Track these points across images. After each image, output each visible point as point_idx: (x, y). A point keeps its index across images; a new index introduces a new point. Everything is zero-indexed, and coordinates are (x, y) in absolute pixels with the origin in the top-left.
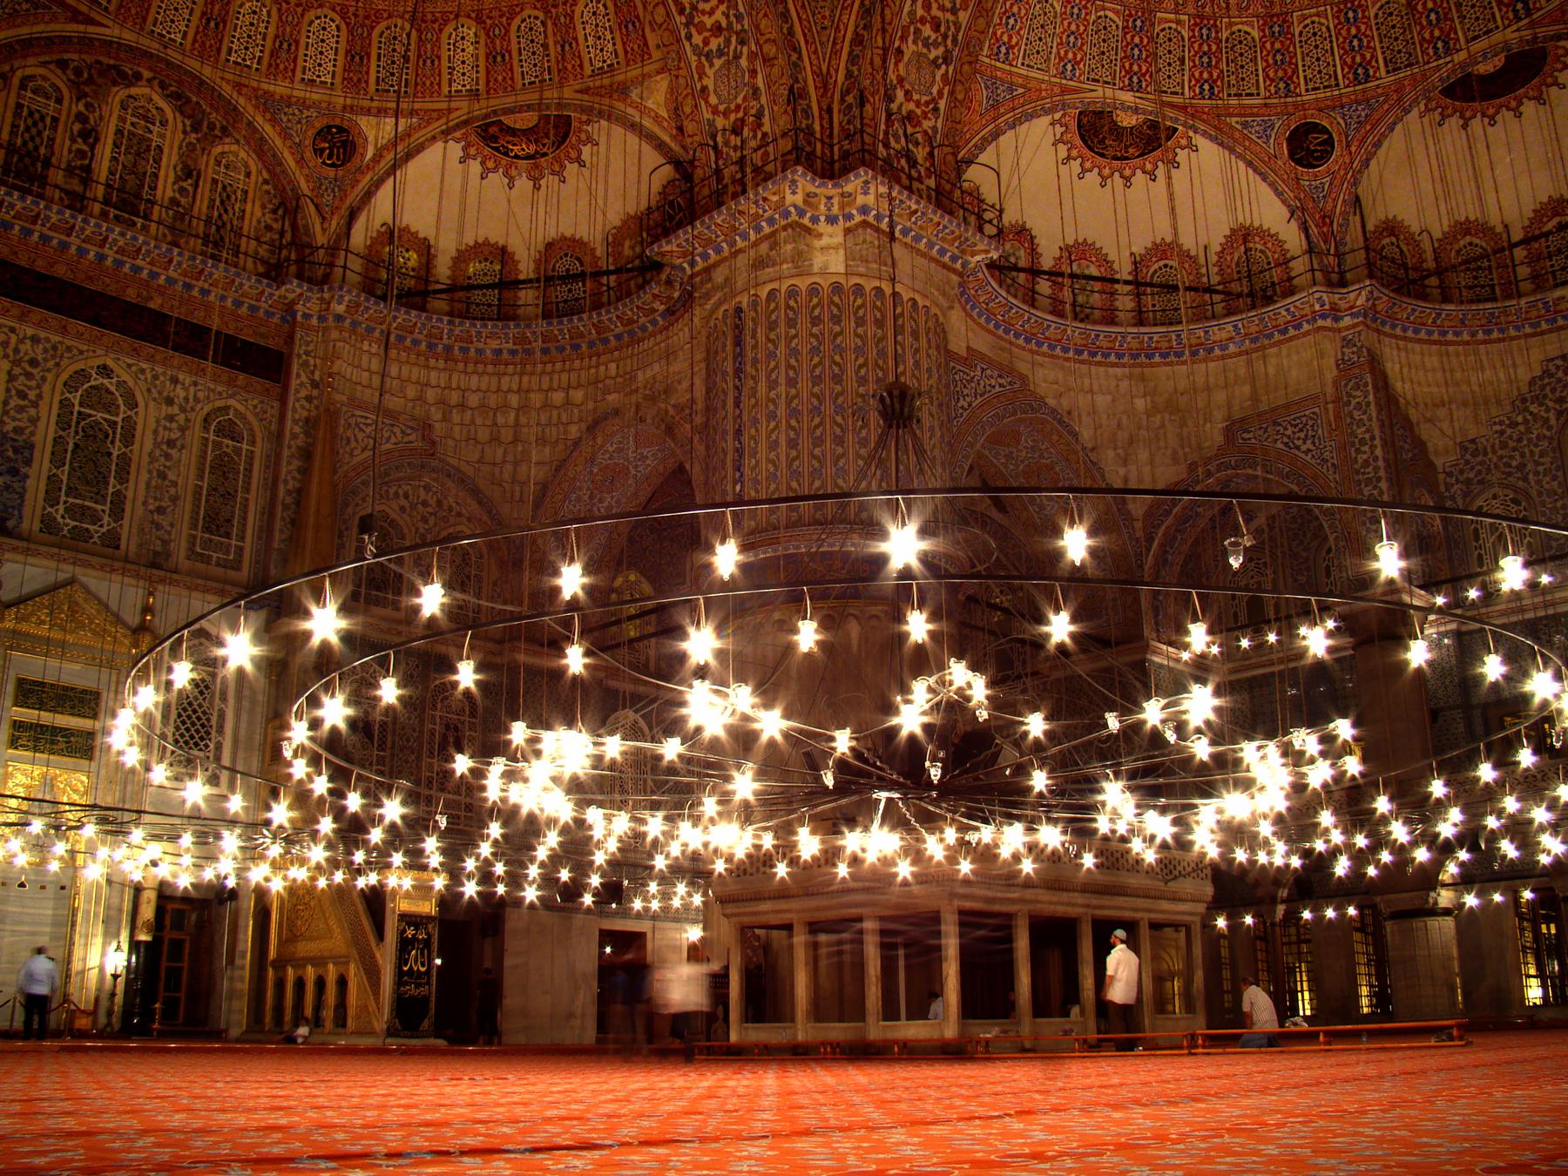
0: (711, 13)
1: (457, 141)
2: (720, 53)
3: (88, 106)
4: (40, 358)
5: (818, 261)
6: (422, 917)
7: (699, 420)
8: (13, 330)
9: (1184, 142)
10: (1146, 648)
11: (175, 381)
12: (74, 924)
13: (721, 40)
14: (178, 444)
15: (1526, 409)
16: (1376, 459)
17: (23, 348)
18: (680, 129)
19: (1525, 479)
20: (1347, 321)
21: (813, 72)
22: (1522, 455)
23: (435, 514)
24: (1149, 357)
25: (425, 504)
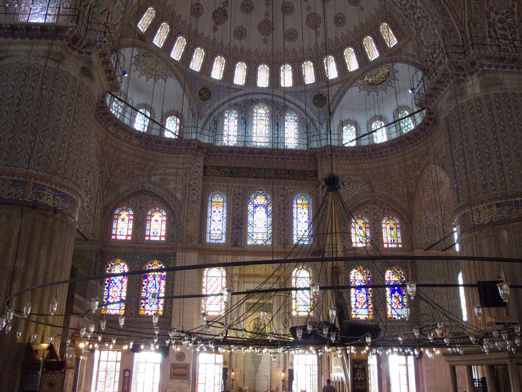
1: (356, 86)
2: (423, 26)
5: (469, 91)
6: (360, 360)
8: (232, 186)
11: (283, 189)
13: (421, 22)
14: (287, 208)
21: (455, 20)
23: (379, 211)
25: (374, 209)
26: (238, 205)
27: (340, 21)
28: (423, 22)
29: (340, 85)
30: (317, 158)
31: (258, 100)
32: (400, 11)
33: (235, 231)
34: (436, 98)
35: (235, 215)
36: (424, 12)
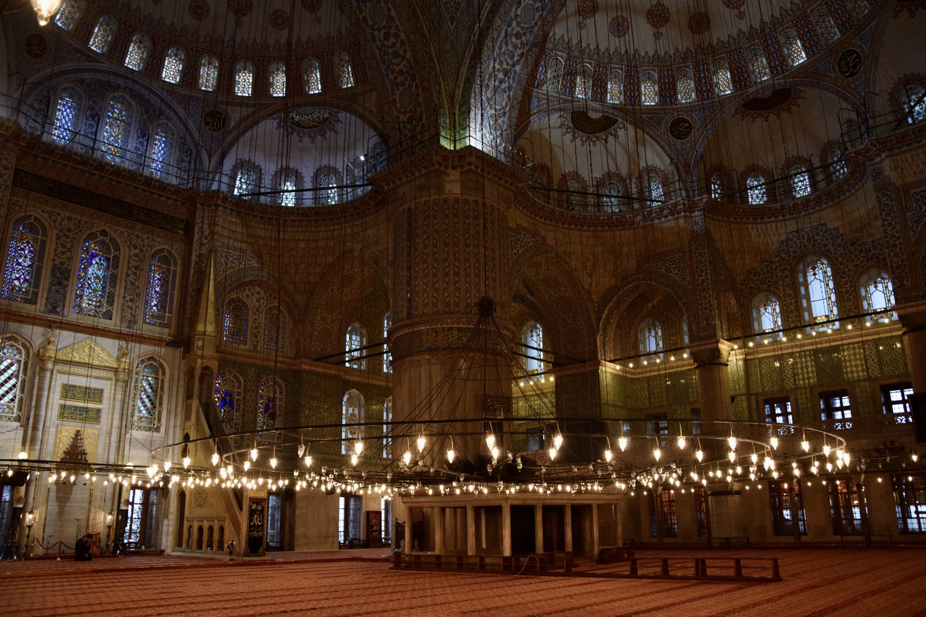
0: (398, 65)
1: (274, 119)
2: (403, 84)
3: (94, 102)
4: (72, 227)
5: (448, 187)
7: (390, 258)
9: (621, 126)
10: (599, 364)
11: (138, 237)
12: (90, 502)
13: (403, 78)
15: (779, 255)
16: (708, 279)
17: (64, 223)
18: (383, 118)
19: (778, 289)
20: (697, 213)
22: (777, 277)
24: (602, 227)
26: (64, 246)
27: (280, 21)
28: (406, 80)
29: (251, 109)
30: (196, 203)
31: (118, 87)
32: (377, 52)
33: (54, 288)
34: (400, 179)
35: (57, 262)
36: (412, 68)
